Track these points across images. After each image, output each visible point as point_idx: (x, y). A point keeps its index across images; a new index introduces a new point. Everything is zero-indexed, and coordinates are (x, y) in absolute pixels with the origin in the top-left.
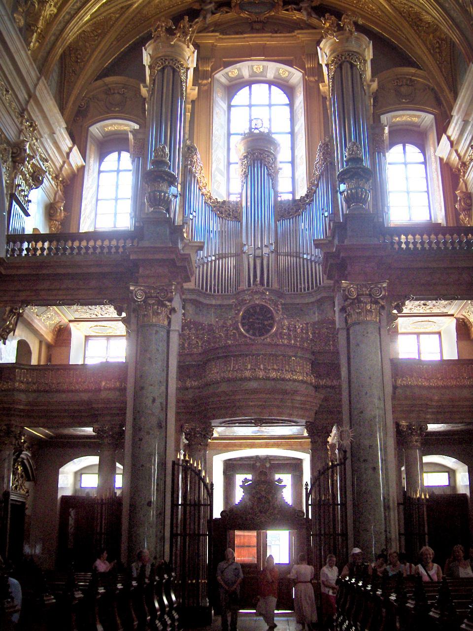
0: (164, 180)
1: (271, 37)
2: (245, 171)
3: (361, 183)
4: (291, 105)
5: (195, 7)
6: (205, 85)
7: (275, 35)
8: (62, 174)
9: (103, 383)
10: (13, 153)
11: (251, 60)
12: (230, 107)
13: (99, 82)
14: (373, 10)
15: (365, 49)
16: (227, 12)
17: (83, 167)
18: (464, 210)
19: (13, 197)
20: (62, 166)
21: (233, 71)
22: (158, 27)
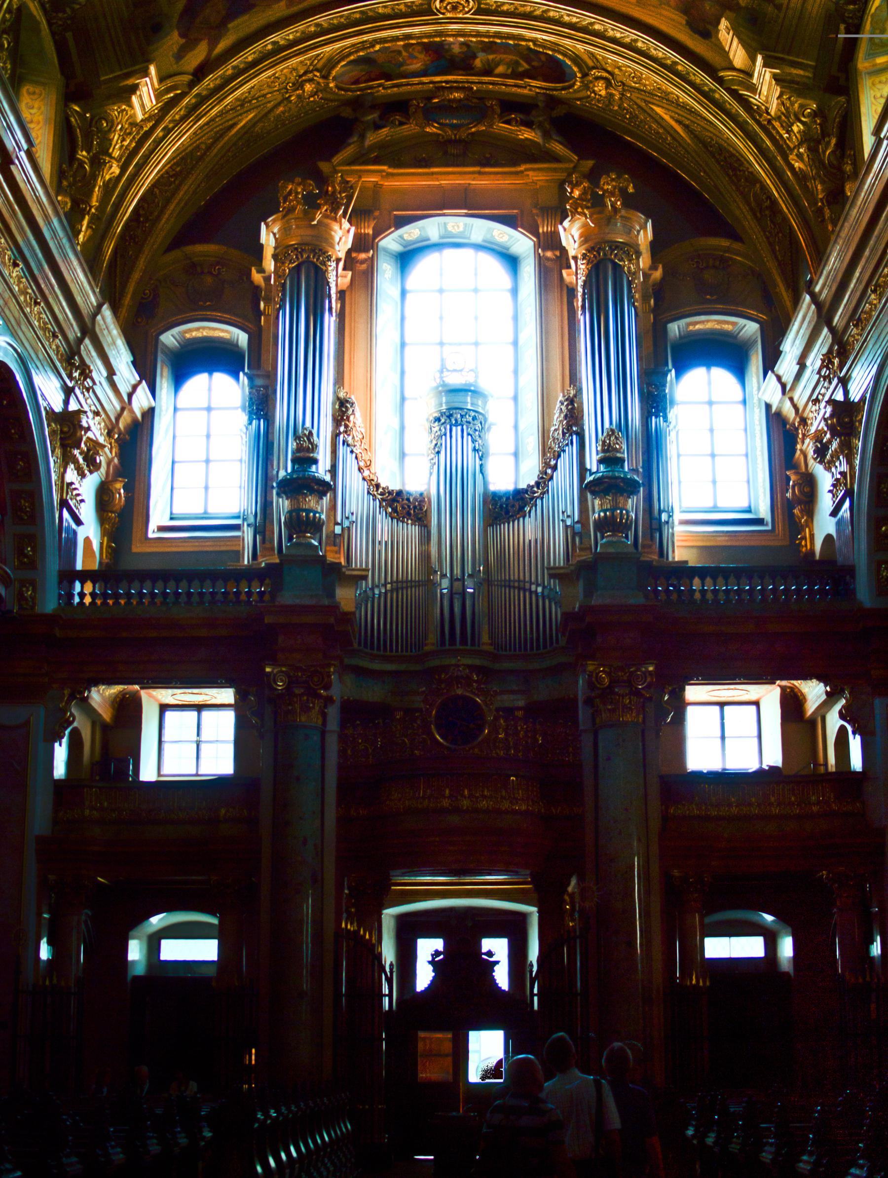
0: (312, 491)
1: (479, 173)
2: (436, 445)
3: (621, 500)
4: (515, 291)
5: (343, 114)
6: (363, 262)
7: (487, 170)
8: (119, 429)
9: (223, 811)
10: (62, 432)
11: (444, 215)
12: (403, 293)
13: (176, 254)
14: (658, 133)
15: (639, 232)
16: (401, 124)
17: (150, 413)
18: (800, 502)
19: (64, 503)
20: (118, 418)
21: (411, 232)
22: (290, 193)
